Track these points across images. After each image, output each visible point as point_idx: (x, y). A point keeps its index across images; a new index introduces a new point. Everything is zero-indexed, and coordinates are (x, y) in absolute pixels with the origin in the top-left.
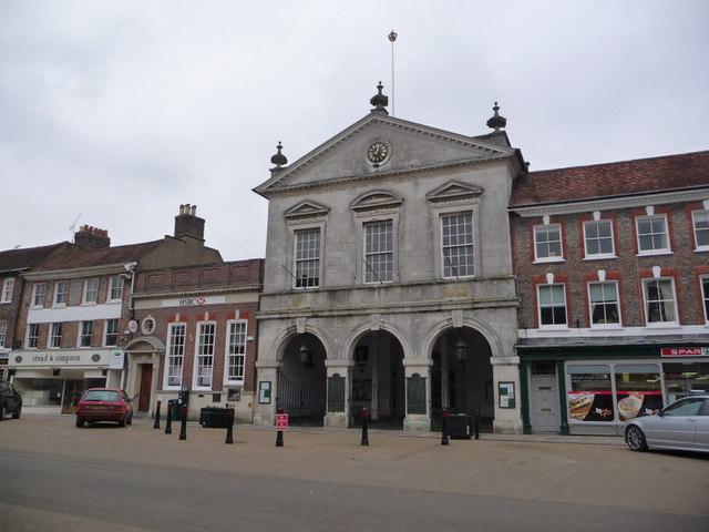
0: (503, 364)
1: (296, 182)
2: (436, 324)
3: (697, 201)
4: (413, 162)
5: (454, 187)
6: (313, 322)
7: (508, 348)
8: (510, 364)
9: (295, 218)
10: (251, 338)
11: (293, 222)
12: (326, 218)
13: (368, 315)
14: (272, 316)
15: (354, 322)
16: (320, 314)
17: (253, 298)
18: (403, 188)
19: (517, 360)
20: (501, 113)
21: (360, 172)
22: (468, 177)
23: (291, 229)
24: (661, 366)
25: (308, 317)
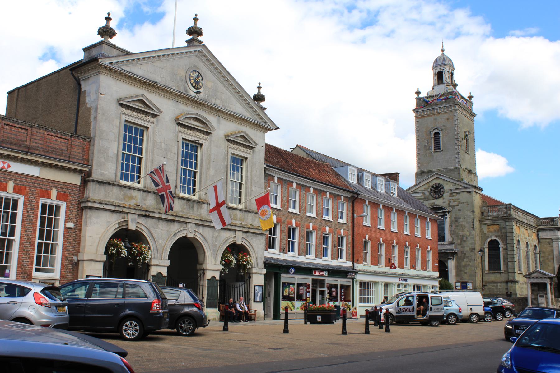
0: (259, 274)
1: (128, 69)
2: (227, 238)
3: (323, 191)
4: (218, 102)
5: (242, 136)
6: (142, 220)
7: (261, 264)
8: (261, 274)
9: (128, 107)
10: (71, 225)
11: (127, 111)
12: (155, 120)
13: (186, 223)
14: (105, 207)
15: (175, 227)
16: (151, 214)
17: (76, 180)
18: (211, 119)
19: (264, 271)
20: (263, 92)
21: (182, 90)
22: (154, 98)
23: (124, 118)
24: (311, 279)
25: (139, 215)
